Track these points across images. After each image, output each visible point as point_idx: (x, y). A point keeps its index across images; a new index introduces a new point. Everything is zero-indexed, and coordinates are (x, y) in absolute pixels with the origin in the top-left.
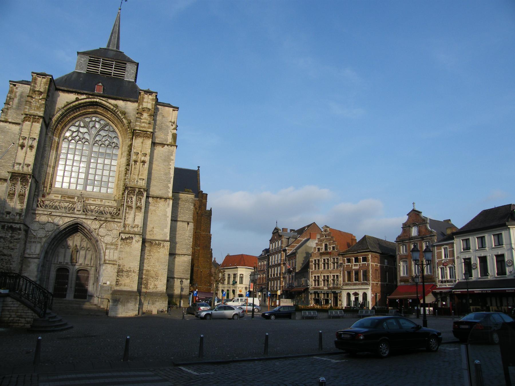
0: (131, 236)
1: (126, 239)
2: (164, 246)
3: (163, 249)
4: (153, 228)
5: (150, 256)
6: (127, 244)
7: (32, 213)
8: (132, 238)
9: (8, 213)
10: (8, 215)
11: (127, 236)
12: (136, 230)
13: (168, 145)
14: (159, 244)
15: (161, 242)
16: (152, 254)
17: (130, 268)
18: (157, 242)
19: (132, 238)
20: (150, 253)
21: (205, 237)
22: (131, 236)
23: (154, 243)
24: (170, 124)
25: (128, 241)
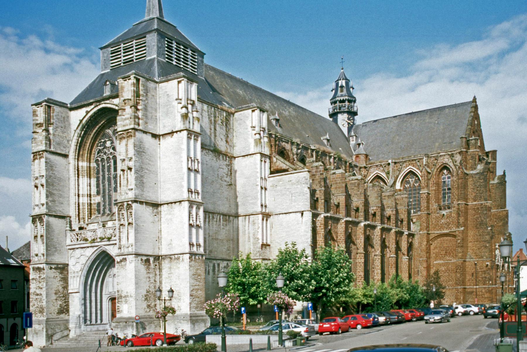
0: (124, 257)
1: (121, 261)
2: (183, 260)
3: (183, 264)
4: (171, 240)
5: (171, 273)
6: (122, 267)
7: (69, 249)
8: (125, 259)
9: (37, 255)
10: (36, 257)
11: (121, 257)
12: (130, 249)
13: (176, 132)
14: (178, 259)
15: (179, 255)
16: (172, 271)
17: (127, 292)
18: (176, 256)
19: (125, 259)
20: (171, 270)
21: (478, 208)
22: (124, 257)
23: (173, 257)
24: (177, 102)
25: (123, 263)
